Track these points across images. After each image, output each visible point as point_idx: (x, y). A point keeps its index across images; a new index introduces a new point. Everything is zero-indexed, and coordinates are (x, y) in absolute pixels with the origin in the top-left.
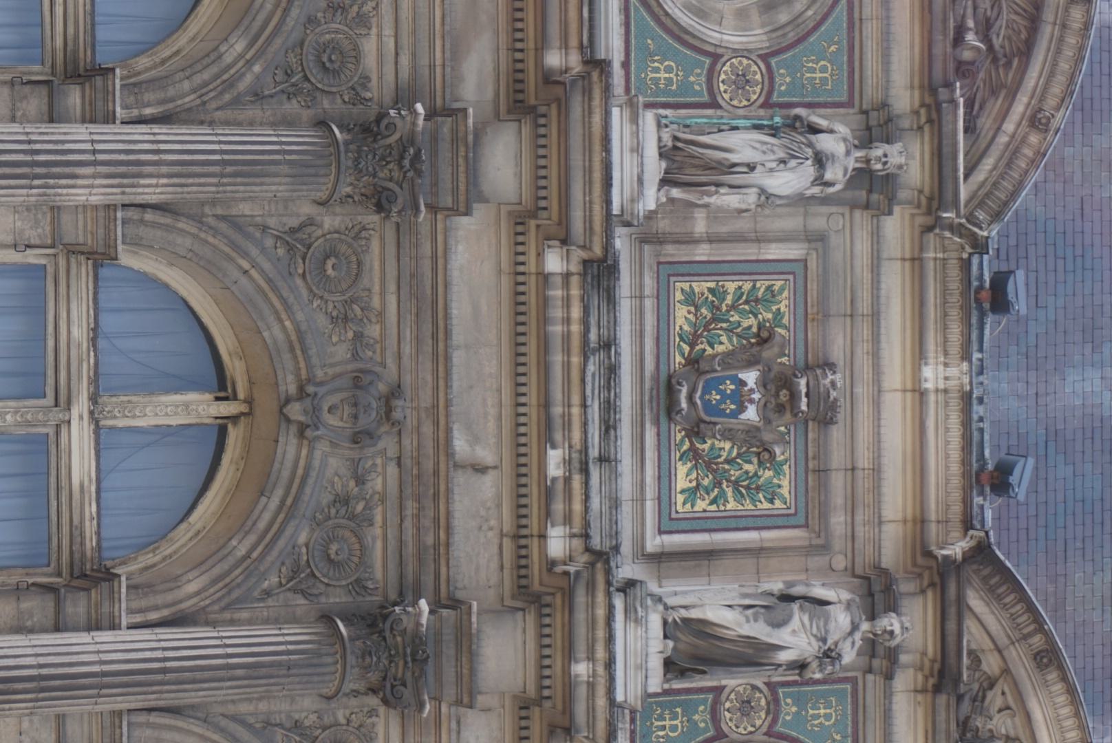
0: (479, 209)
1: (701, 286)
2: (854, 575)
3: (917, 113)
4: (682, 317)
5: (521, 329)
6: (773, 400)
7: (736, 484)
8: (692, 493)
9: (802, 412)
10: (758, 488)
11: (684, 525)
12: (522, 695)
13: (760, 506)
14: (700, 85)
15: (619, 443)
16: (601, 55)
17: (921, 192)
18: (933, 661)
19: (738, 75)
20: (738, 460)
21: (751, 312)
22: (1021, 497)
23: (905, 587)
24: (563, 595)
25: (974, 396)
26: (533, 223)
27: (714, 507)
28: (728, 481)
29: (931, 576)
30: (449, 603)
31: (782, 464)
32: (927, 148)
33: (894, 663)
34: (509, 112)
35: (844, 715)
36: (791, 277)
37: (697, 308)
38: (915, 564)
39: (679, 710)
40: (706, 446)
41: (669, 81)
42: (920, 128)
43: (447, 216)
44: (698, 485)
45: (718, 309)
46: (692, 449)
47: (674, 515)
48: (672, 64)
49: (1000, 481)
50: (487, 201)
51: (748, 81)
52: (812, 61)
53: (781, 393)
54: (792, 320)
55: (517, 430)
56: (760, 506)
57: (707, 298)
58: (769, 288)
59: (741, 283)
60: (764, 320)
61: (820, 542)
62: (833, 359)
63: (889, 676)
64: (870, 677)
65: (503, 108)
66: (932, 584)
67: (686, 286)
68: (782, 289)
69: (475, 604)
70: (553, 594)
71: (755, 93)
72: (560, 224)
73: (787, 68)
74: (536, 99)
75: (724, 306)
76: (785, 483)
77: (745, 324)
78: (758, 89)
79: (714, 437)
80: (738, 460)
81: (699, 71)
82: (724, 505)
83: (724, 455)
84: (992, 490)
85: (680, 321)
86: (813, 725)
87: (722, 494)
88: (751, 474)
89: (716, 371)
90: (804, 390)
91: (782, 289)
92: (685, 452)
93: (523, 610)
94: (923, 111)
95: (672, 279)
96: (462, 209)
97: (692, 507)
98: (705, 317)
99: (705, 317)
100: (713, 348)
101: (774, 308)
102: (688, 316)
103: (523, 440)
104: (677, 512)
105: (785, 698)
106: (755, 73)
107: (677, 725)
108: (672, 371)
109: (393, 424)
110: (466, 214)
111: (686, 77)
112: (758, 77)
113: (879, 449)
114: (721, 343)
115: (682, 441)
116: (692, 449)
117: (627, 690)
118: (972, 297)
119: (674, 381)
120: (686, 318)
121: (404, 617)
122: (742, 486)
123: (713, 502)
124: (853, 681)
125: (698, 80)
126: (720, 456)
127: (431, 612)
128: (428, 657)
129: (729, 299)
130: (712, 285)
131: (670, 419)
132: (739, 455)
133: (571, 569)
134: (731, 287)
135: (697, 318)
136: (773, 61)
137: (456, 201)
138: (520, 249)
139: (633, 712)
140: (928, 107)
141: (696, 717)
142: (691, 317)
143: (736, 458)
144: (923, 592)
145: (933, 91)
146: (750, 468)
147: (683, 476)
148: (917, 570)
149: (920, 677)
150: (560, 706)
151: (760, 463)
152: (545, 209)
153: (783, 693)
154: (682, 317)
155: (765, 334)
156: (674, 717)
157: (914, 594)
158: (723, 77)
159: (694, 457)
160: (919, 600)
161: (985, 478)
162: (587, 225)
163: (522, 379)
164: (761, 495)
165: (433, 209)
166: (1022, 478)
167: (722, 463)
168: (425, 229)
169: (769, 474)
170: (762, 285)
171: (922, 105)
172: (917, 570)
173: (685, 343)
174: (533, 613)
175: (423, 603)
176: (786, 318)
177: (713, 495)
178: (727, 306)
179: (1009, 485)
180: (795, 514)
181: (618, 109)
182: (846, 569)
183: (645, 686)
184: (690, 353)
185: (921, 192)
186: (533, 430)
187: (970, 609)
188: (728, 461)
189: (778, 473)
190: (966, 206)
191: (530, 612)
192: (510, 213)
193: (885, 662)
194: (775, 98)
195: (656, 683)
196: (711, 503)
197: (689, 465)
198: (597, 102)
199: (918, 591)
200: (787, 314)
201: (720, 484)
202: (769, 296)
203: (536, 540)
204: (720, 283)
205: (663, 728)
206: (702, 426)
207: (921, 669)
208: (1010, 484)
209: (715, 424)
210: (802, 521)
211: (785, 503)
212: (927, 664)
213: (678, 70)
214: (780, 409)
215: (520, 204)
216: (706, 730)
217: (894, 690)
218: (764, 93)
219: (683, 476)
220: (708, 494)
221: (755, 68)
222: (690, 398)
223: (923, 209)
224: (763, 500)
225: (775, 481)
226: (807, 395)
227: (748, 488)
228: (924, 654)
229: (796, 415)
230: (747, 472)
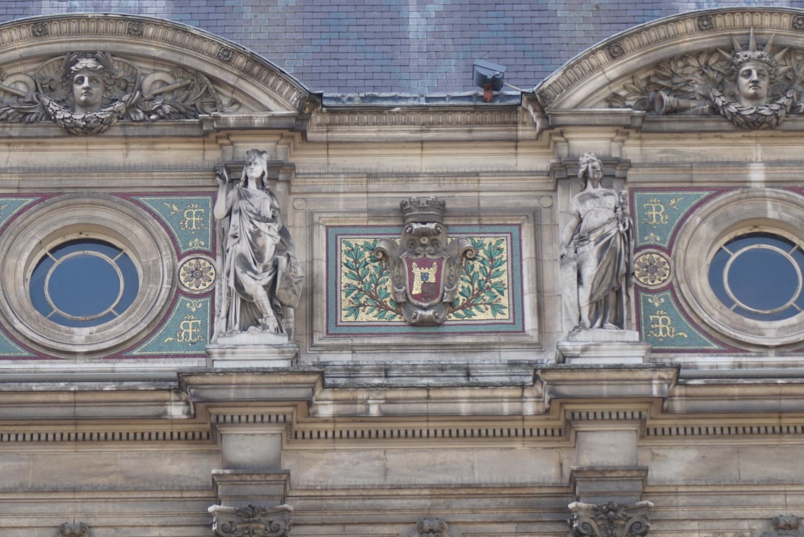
0: (287, 464)
1: (345, 302)
2: (555, 190)
3: (221, 145)
4: (367, 316)
5: (153, 436)
6: (427, 249)
7: (489, 276)
8: (496, 308)
9: (436, 227)
10: (491, 259)
11: (519, 316)
12: (639, 432)
13: (504, 259)
14: (199, 303)
15: (336, 364)
16: (175, 375)
17: (277, 143)
18: (617, 132)
19: (192, 276)
20: (471, 274)
21: (364, 267)
22: (503, 69)
23: (564, 151)
24: (210, 407)
25: (425, 103)
26: (296, 427)
27: (506, 292)
28: (486, 282)
29: (556, 134)
30: (572, 486)
31: (474, 244)
32: (242, 138)
33: (283, 164)
34: (215, 443)
35: (197, 202)
36: (339, 237)
37: (360, 305)
38: (548, 147)
39: (651, 317)
40: (461, 298)
41: (195, 326)
42: (232, 143)
43: (291, 489)
44: (490, 304)
45: (360, 290)
46: (462, 308)
47: (511, 321)
48: (183, 322)
49: (492, 84)
50: (280, 459)
51: (196, 269)
52: (184, 223)
53: (423, 242)
54: (370, 237)
55: (65, 441)
56: (504, 259)
57: (353, 298)
58: (348, 253)
59: (343, 274)
60: (370, 257)
61: (531, 215)
62: (397, 205)
63: (629, 165)
64: (629, 179)
65: (213, 447)
66: (562, 134)
67: (344, 313)
68: (348, 245)
69: (214, 471)
70: (565, 411)
71: (204, 263)
72: (295, 406)
73: (188, 242)
74: (206, 423)
75: (359, 287)
76: (486, 241)
77: (372, 270)
78: (202, 261)
79: (454, 292)
80: (471, 274)
81: (188, 305)
82: (504, 285)
83: (466, 285)
84: (498, 90)
85: (371, 317)
86: (664, 220)
87: (495, 285)
88: (482, 265)
89: (405, 291)
90: (420, 226)
91: (348, 245)
92: (465, 313)
93: (576, 432)
94: (220, 141)
95: (339, 323)
96: (284, 477)
97: (506, 308)
98: (367, 299)
99: (367, 299)
100: (390, 294)
101: (362, 249)
102: (366, 312)
103: (461, 433)
104: (341, 321)
105: (189, 247)
106: (191, 264)
107: (193, 323)
108: (403, 324)
109: (442, 528)
110: (289, 474)
111: (191, 313)
112: (193, 262)
113: (359, 173)
114: (463, 287)
115: (457, 316)
116: (462, 308)
117: (636, 356)
118: (489, 104)
119: (414, 321)
120: (367, 314)
121: (221, 523)
122: (358, 273)
123: (502, 293)
124: (632, 191)
125: (194, 306)
126: (468, 288)
127: (578, 500)
128: (250, 506)
129: (355, 283)
130: (344, 294)
131: (439, 325)
132: (468, 274)
133: (547, 397)
134: (345, 280)
135: (368, 305)
136: (183, 251)
137: (277, 482)
138: (315, 435)
139: (653, 351)
140: (217, 138)
141: (657, 304)
142: (368, 308)
143: (470, 276)
144: (567, 141)
145: (206, 134)
146: (477, 265)
147: (482, 315)
148: (552, 144)
149: (629, 142)
150: (645, 406)
151: (474, 259)
152: (285, 417)
153: (184, 248)
154: (367, 316)
155: (380, 255)
156: (657, 321)
157: (568, 146)
158: (193, 287)
159: (469, 306)
160: (572, 142)
161: (488, 96)
162: (283, 386)
163: (395, 433)
164: (497, 258)
165: (284, 498)
166: (491, 68)
167: (473, 288)
168: (299, 503)
169: (481, 252)
170: (344, 258)
171: (216, 142)
172: (552, 144)
173: (385, 314)
174: (222, 429)
175: (572, 505)
176: (368, 240)
177: (497, 293)
178: (359, 284)
179: (494, 78)
180: (511, 233)
181: (215, 362)
182: (551, 197)
183: (634, 343)
184: (392, 310)
185: (277, 143)
186: (360, 426)
187: (576, 107)
188: (472, 283)
189: (482, 245)
190: (289, 110)
191: (223, 431)
192: (288, 442)
193: (618, 168)
194: (209, 249)
195: (633, 335)
196: (503, 294)
197: (474, 310)
198: (205, 380)
199: (566, 144)
200: (366, 240)
201: (488, 288)
202: (353, 253)
203: (526, 423)
204: (343, 289)
205: (665, 331)
206: (445, 300)
207: (623, 141)
208: (493, 77)
209: (444, 291)
210: (517, 228)
211: (503, 240)
212: (619, 138)
213: (187, 320)
214: (434, 243)
215: (281, 434)
216: (666, 297)
217: (122, 165)
218: (204, 257)
219: (482, 315)
220: (496, 296)
221: (187, 265)
222: (425, 309)
223: (290, 140)
224: (500, 256)
225: (486, 248)
226: (424, 223)
227: (492, 267)
228: (612, 140)
229: (439, 232)
230: (481, 268)
